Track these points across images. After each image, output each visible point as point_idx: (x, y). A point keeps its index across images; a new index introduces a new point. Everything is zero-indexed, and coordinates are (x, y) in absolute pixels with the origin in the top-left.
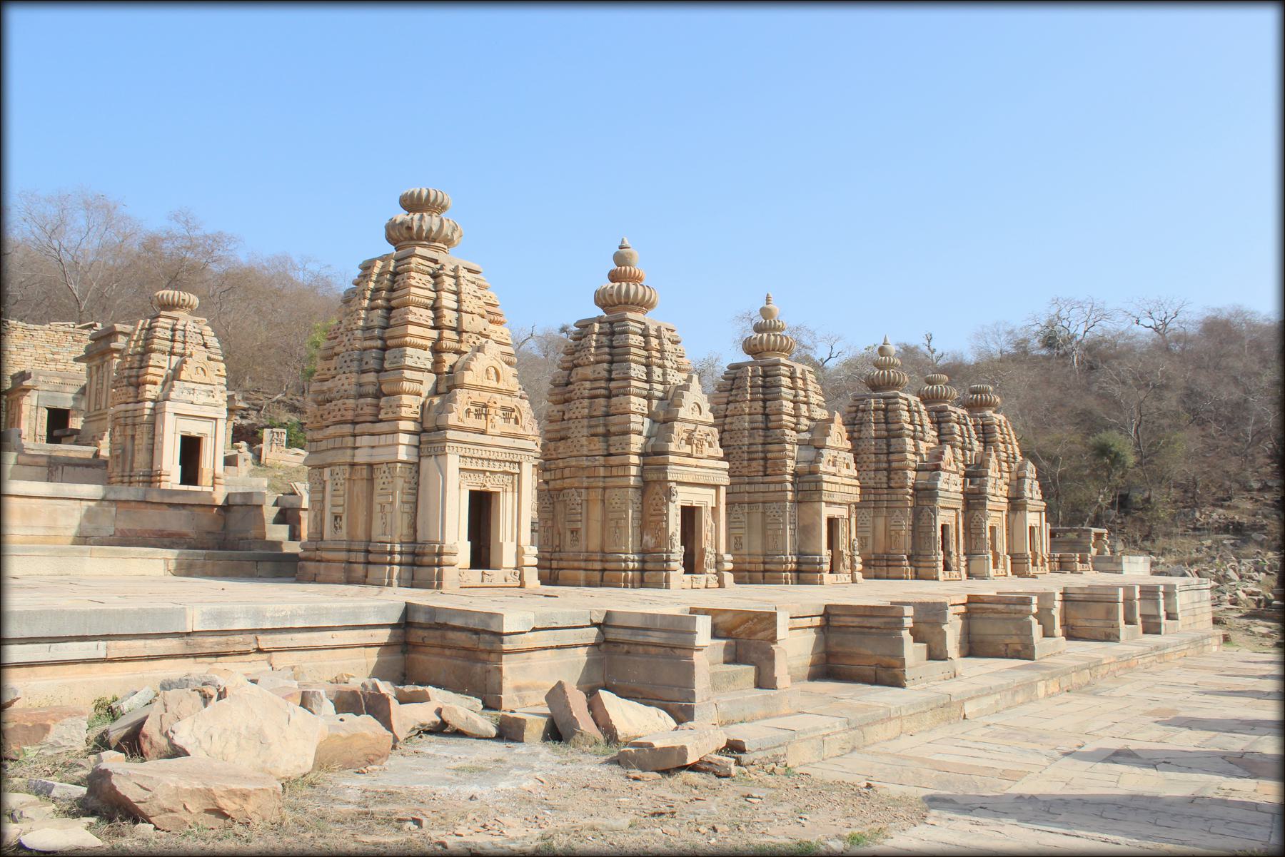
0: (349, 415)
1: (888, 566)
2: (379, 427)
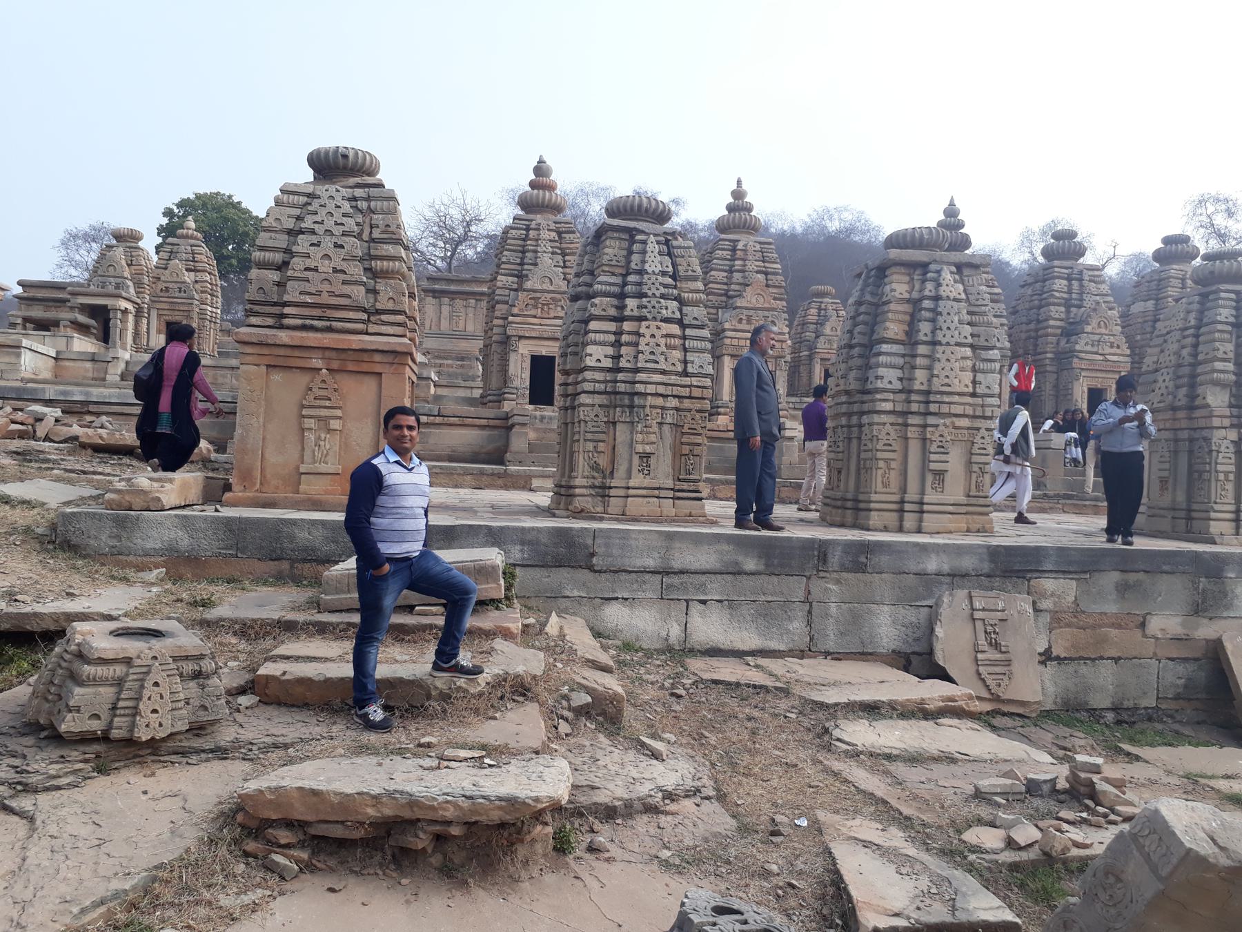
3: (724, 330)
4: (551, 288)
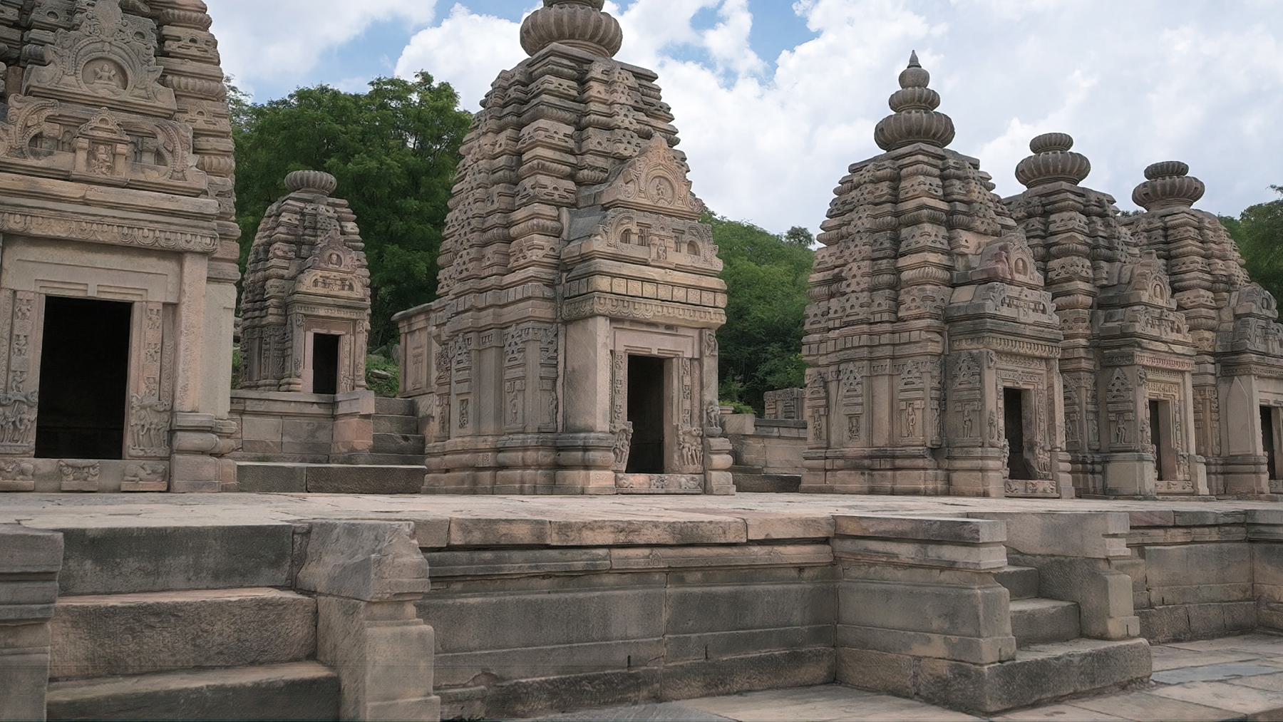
1: (895, 469)
3: (586, 258)
4: (125, 96)
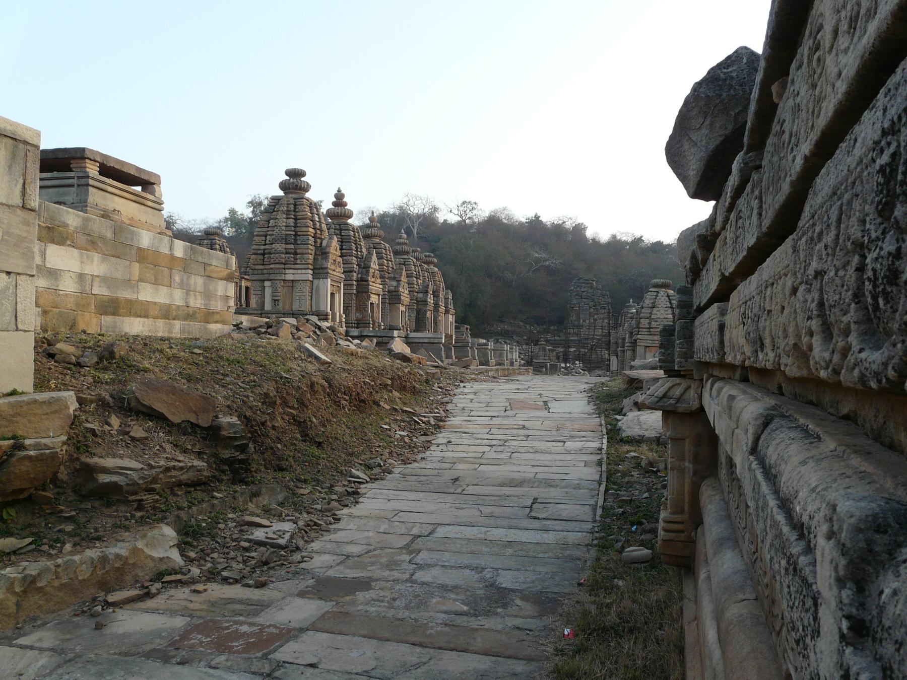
0: (283, 261)
2: (297, 266)
